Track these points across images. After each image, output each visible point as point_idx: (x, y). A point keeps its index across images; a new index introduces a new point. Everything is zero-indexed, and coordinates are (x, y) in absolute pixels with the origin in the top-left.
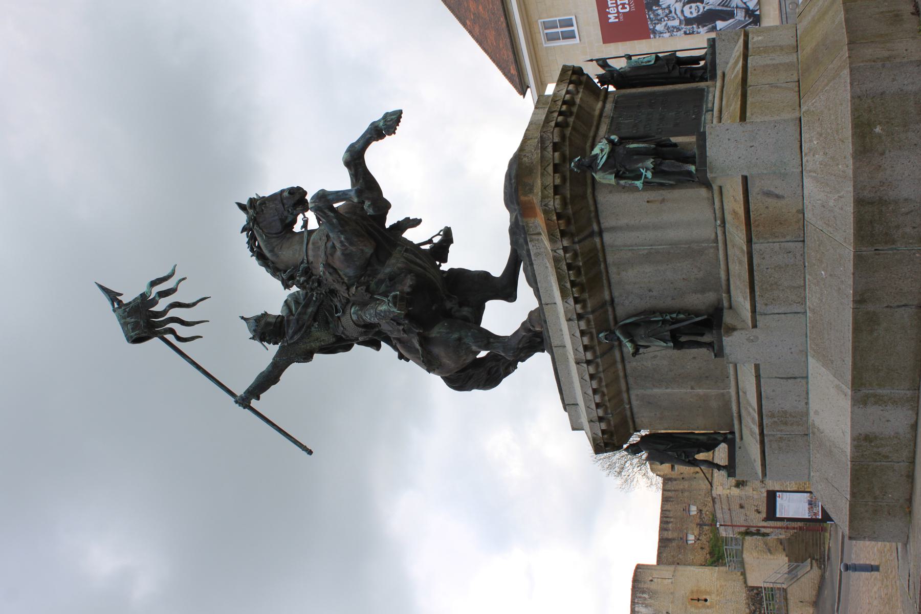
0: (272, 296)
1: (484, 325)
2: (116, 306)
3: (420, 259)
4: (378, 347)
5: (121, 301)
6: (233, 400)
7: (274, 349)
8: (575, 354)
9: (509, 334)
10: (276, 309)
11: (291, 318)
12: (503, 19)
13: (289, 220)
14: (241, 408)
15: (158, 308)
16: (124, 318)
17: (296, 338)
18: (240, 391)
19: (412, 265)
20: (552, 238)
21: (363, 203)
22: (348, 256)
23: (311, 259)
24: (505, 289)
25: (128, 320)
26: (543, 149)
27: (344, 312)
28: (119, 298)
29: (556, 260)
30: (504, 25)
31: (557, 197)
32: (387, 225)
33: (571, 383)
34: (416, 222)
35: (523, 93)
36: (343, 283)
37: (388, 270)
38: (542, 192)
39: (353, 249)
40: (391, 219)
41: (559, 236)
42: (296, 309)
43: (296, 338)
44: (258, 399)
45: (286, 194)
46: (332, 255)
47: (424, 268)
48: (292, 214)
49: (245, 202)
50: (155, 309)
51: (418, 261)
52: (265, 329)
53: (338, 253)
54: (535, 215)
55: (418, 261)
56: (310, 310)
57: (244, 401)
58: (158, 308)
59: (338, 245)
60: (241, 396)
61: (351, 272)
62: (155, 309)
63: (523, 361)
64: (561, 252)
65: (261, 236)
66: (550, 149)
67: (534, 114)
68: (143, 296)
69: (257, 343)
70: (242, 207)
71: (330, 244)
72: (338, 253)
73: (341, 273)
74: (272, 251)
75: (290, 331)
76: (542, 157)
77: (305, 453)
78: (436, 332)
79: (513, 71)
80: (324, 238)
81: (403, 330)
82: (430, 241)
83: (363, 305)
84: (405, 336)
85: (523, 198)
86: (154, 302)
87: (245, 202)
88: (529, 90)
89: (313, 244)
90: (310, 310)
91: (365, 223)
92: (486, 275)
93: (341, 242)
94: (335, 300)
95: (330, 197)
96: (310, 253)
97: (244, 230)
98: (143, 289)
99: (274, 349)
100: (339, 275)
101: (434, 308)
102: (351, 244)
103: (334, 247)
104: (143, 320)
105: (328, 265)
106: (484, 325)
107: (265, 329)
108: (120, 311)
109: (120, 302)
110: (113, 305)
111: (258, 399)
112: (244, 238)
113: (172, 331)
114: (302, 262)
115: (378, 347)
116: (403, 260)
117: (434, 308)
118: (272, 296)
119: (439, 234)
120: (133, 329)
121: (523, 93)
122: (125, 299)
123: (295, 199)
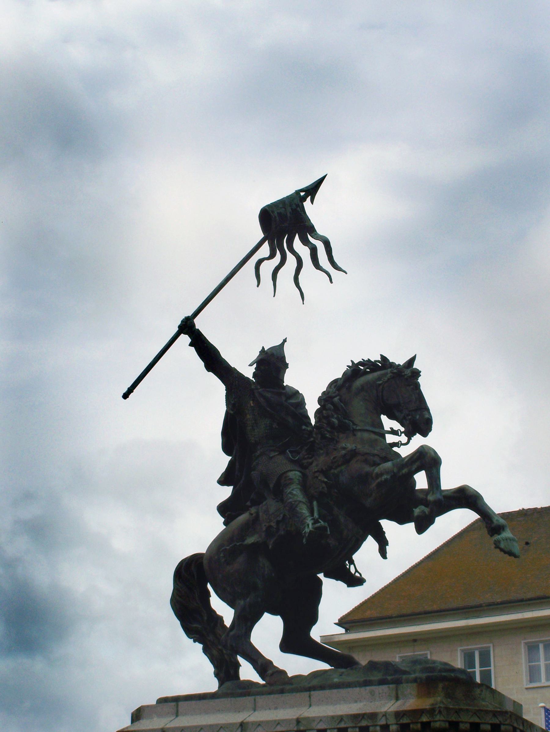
0: (309, 380)
1: (266, 615)
2: (302, 194)
4: (224, 481)
5: (305, 201)
6: (190, 314)
7: (248, 372)
8: (253, 723)
9: (251, 641)
10: (291, 379)
11: (284, 399)
12: (435, 607)
13: (397, 414)
14: (179, 323)
15: (297, 243)
16: (291, 205)
17: (261, 400)
18: (199, 323)
20: (398, 715)
21: (426, 506)
22: (364, 479)
23: (359, 434)
24: (296, 640)
25: (289, 210)
26: (495, 714)
27: (292, 461)
28: (309, 199)
29: (373, 716)
30: (428, 608)
31: (447, 725)
32: (381, 521)
33: (207, 712)
34: (383, 553)
35: (341, 623)
36: (331, 468)
37: (342, 519)
38: (452, 709)
39: (374, 485)
40: (387, 525)
41: (401, 721)
42: (292, 404)
43: (261, 400)
44: (191, 345)
45: (427, 416)
46: (366, 461)
48: (404, 418)
49: (416, 365)
50: (297, 239)
52: (272, 363)
53: (367, 469)
54: (420, 695)
56: (290, 419)
57: (187, 326)
58: (297, 243)
59: (377, 470)
60: (194, 325)
61: (343, 479)
62: (297, 239)
63: (283, 673)
64: (383, 722)
65: (379, 379)
66: (495, 721)
67: (509, 699)
68: (311, 230)
69: (255, 355)
70: (412, 361)
71: (377, 459)
72: (367, 469)
73: (343, 467)
74: (362, 389)
75: (268, 395)
76: (487, 712)
77: (125, 390)
78: (264, 564)
79: (368, 614)
80: (383, 455)
81: (270, 527)
83: (305, 487)
84: (264, 529)
85: (441, 685)
86: (305, 242)
87: (416, 365)
88: (342, 630)
89: (376, 440)
90: (290, 419)
92: (313, 618)
93: (381, 474)
94: (304, 452)
95: (434, 471)
96: (366, 435)
97: (383, 357)
98: (320, 230)
99: (248, 372)
100: (339, 466)
102: (379, 485)
103: (376, 464)
104: (285, 222)
105: (354, 454)
106: (266, 615)
107: (272, 363)
108: (297, 201)
109: (304, 199)
110: (302, 190)
111: (191, 345)
112: (375, 357)
113: (272, 256)
114: (354, 424)
115: (224, 481)
118: (309, 380)
119: (356, 571)
120: (280, 214)
121: (341, 623)
122: (307, 204)
123: (419, 421)
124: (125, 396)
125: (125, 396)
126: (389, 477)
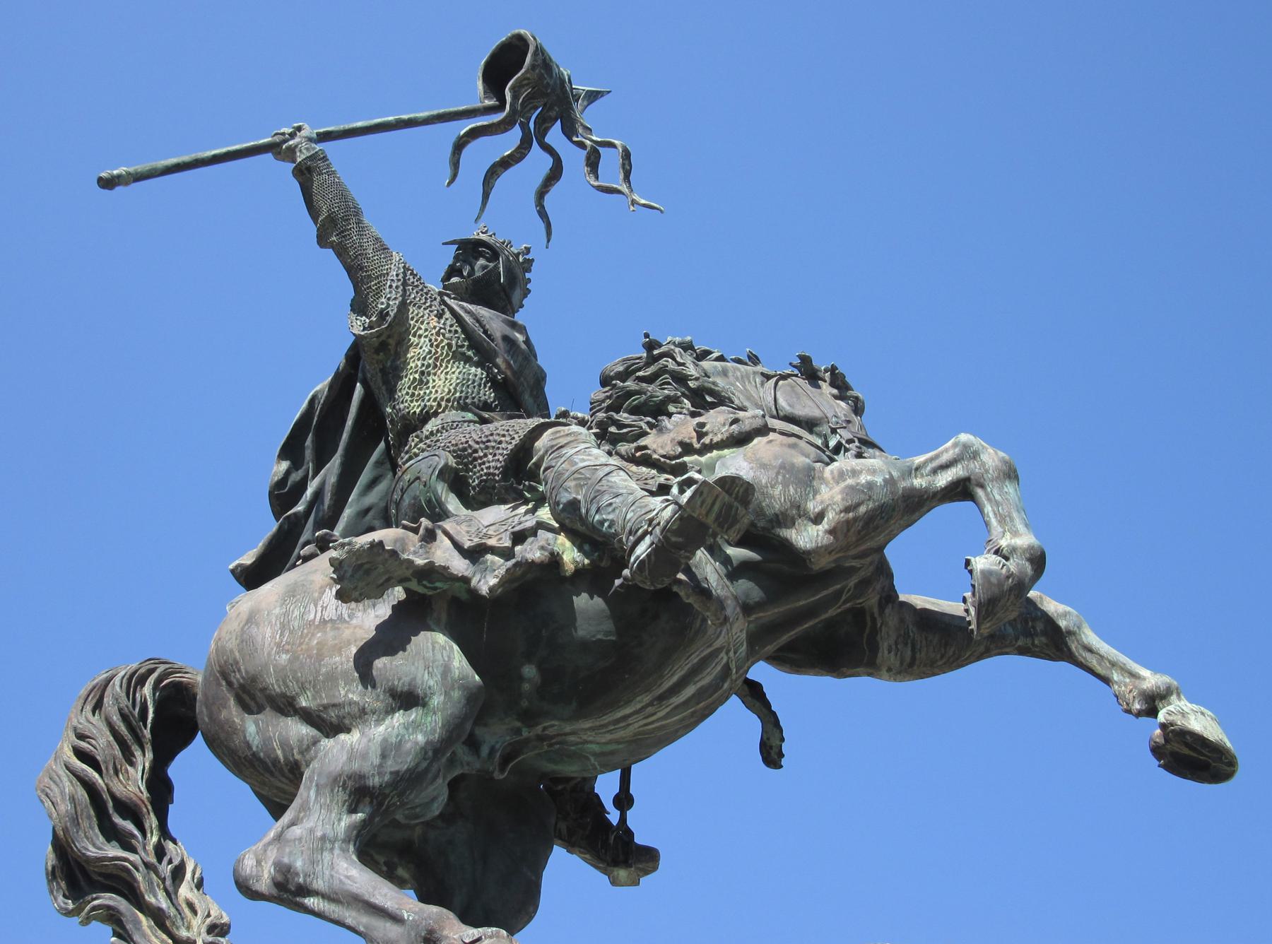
3: (686, 703)
19: (695, 659)
47: (662, 698)
51: (690, 691)
55: (690, 691)
82: (624, 800)
91: (852, 582)
101: (530, 671)
116: (717, 644)
117: (530, 671)
124: (108, 183)
125: (108, 183)
126: (879, 480)
